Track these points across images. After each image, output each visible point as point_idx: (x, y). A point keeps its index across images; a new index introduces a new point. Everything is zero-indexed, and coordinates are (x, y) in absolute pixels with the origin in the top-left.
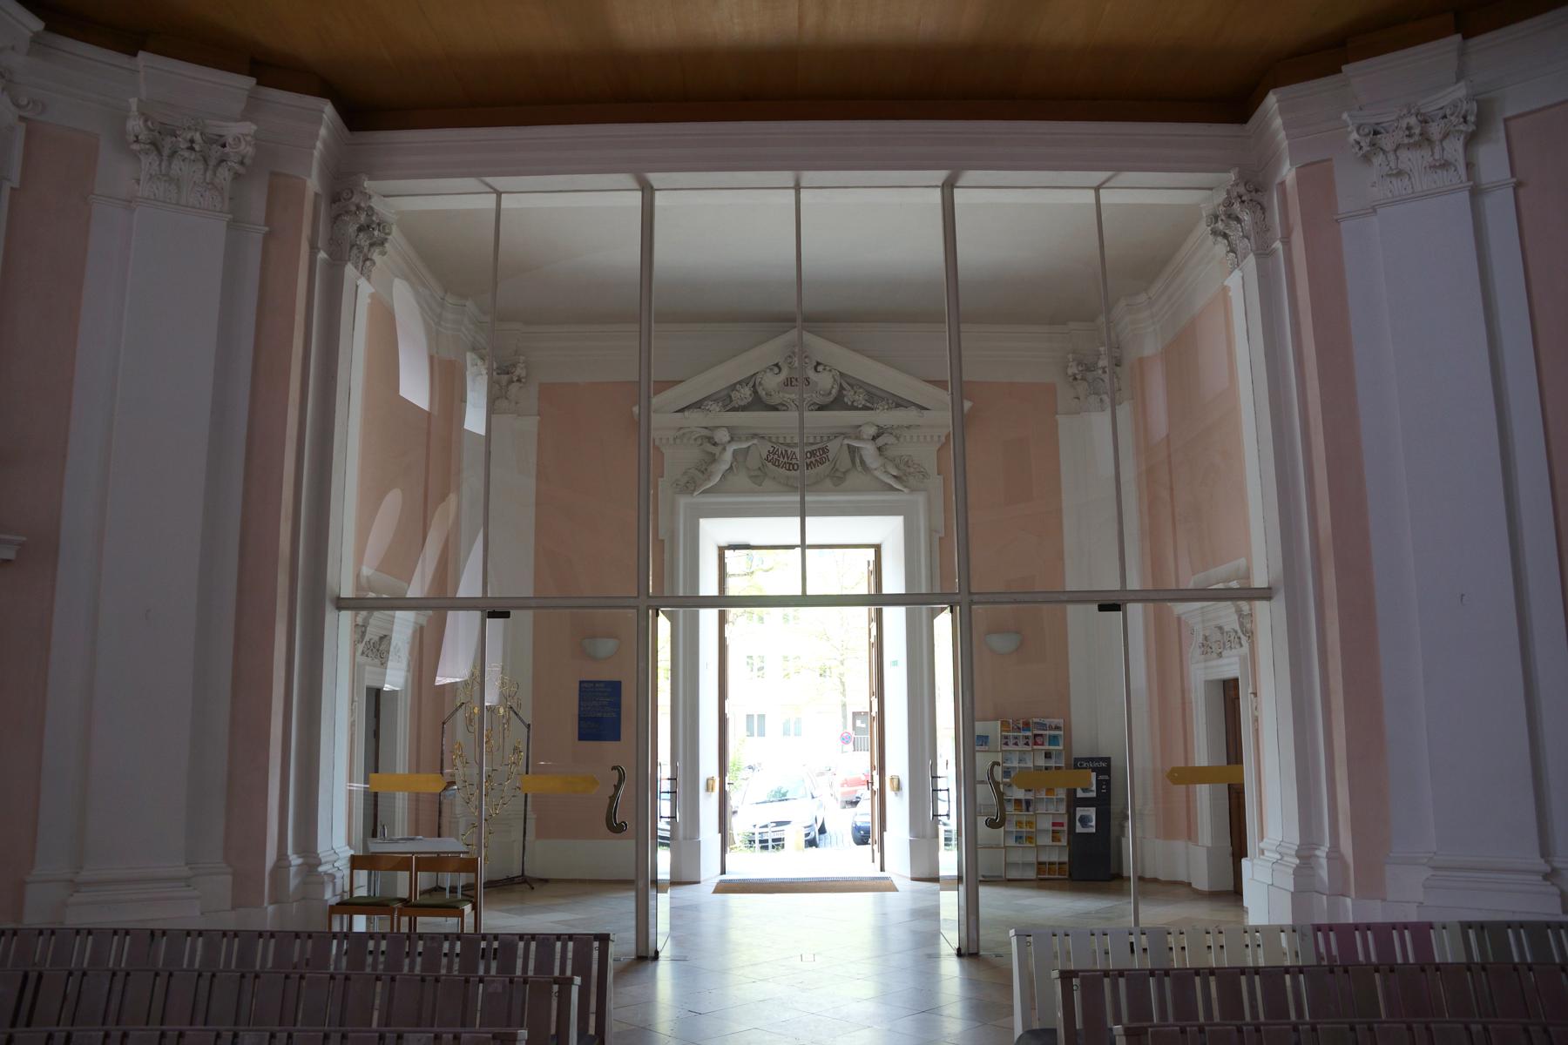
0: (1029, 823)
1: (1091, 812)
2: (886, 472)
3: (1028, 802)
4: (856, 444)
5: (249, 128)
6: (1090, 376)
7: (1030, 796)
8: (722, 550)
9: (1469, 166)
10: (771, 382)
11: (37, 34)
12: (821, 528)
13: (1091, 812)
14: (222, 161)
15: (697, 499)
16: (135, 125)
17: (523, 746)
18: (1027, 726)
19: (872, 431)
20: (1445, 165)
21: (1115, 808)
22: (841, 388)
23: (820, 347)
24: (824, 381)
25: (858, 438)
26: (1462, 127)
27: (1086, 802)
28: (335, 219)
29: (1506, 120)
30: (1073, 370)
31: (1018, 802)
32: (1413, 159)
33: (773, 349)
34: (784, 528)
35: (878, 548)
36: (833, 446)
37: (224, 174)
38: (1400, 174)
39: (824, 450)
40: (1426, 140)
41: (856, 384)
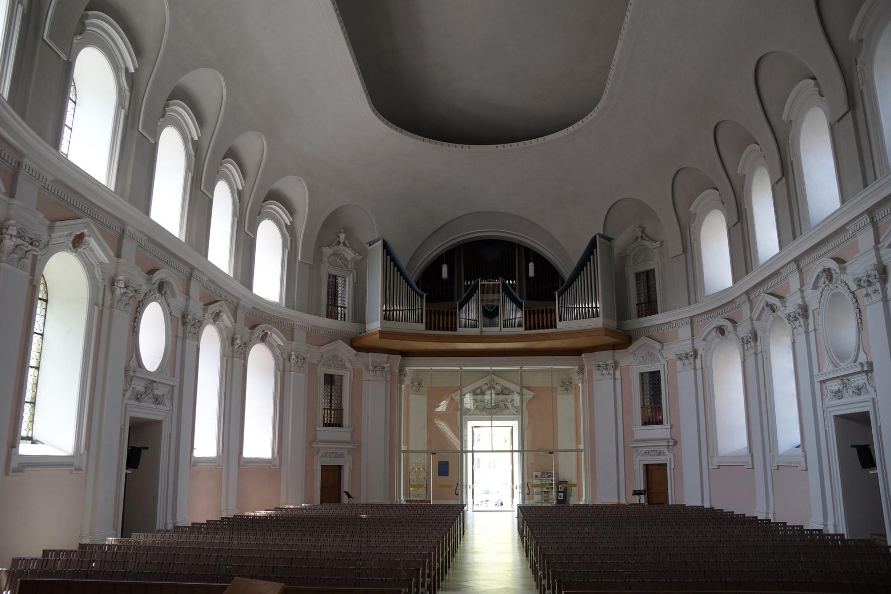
0: (548, 497)
1: (562, 494)
2: (514, 411)
3: (547, 492)
4: (506, 403)
5: (388, 365)
6: (565, 385)
7: (548, 490)
8: (473, 427)
9: (614, 374)
10: (485, 387)
11: (356, 354)
12: (495, 423)
13: (562, 494)
14: (384, 371)
15: (467, 416)
16: (371, 367)
17: (426, 478)
18: (547, 473)
19: (510, 400)
20: (610, 374)
21: (568, 493)
22: (503, 389)
23: (498, 379)
24: (498, 387)
25: (507, 402)
26: (612, 368)
27: (561, 492)
28: (400, 375)
29: (621, 367)
30: (560, 384)
31: (545, 492)
32: (605, 372)
33: (486, 380)
34: (488, 423)
35: (512, 427)
36: (501, 404)
37: (384, 373)
38: (603, 375)
39: (498, 405)
40: (607, 369)
41: (506, 388)
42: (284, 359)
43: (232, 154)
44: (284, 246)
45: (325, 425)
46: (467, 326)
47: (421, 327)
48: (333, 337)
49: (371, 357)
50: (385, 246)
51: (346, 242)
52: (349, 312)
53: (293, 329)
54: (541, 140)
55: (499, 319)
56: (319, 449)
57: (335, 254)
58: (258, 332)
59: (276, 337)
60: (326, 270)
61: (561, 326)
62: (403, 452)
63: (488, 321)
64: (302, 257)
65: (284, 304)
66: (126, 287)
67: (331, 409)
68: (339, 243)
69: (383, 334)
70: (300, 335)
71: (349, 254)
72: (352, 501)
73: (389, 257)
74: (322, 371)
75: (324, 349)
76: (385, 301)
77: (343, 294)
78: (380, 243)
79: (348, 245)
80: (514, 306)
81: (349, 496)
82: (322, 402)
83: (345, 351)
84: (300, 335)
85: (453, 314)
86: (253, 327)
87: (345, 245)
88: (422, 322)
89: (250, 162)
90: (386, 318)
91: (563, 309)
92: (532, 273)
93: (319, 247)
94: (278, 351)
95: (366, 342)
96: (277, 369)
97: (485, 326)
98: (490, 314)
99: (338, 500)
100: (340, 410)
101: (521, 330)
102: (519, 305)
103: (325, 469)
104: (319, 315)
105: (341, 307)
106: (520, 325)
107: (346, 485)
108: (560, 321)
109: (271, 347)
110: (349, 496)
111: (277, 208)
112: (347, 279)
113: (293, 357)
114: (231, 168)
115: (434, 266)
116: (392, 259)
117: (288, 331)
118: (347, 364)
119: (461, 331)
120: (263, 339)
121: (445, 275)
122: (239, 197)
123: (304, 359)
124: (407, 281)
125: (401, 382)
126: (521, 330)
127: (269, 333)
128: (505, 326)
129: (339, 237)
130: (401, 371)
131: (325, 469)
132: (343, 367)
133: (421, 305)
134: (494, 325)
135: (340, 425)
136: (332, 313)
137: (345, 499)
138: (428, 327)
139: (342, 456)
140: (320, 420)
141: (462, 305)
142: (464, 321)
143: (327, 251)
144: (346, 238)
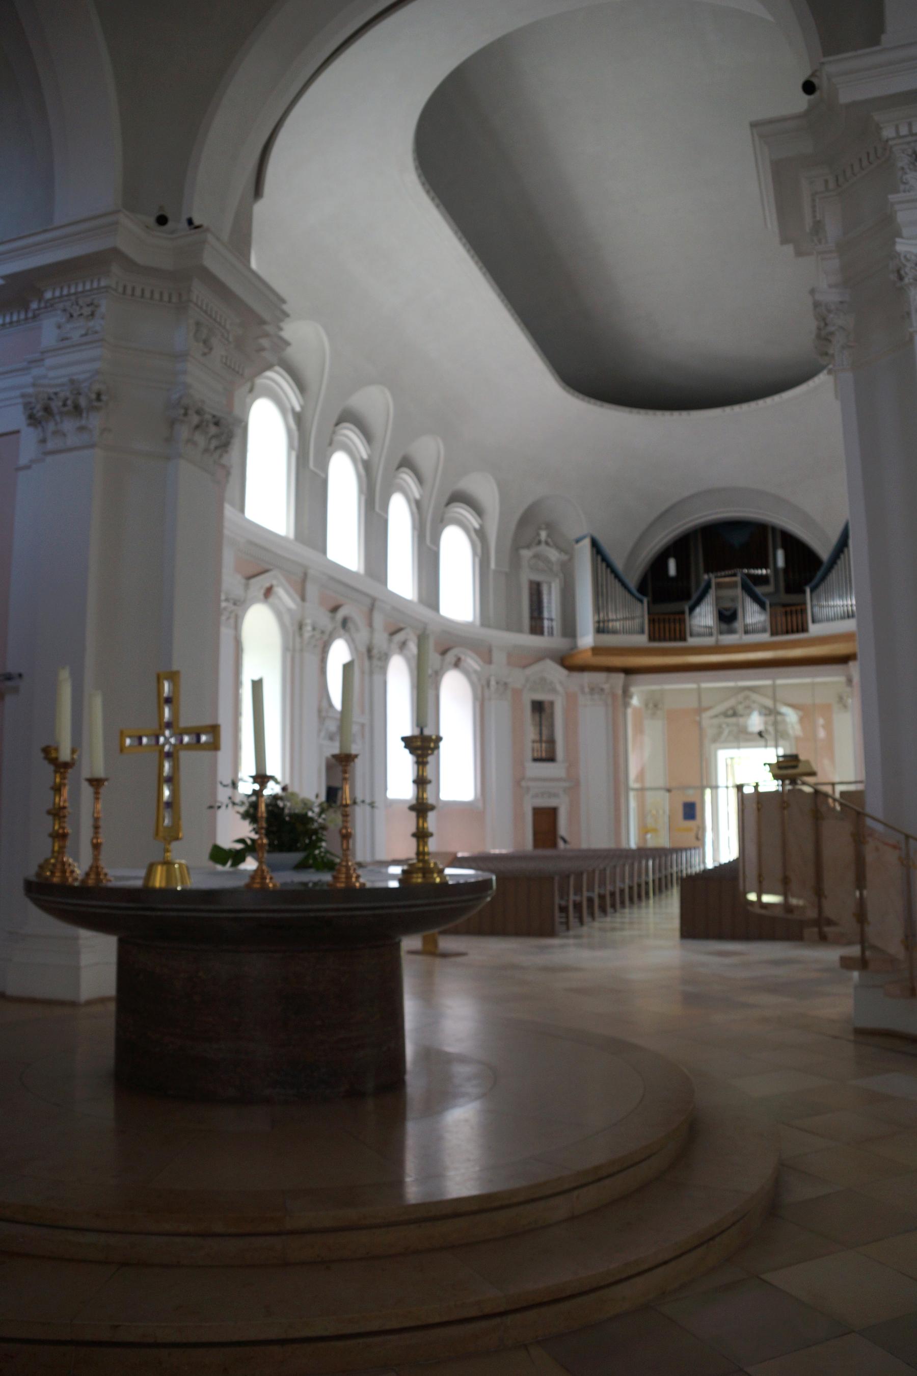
16: (587, 690)
23: (755, 696)
33: (740, 697)
42: (483, 687)
43: (406, 463)
44: (475, 553)
45: (535, 760)
46: (699, 635)
47: (642, 640)
48: (540, 656)
49: (587, 678)
50: (595, 544)
51: (549, 540)
52: (557, 625)
53: (490, 651)
54: (777, 398)
55: (738, 625)
56: (528, 789)
57: (536, 556)
58: (450, 657)
59: (472, 662)
60: (526, 576)
61: (814, 629)
62: (633, 789)
63: (724, 627)
64: (497, 564)
65: (478, 622)
66: (314, 629)
67: (541, 741)
68: (539, 543)
69: (596, 650)
70: (499, 657)
71: (553, 555)
72: (568, 846)
73: (599, 558)
74: (528, 698)
75: (529, 671)
76: (597, 609)
77: (549, 602)
78: (587, 542)
79: (551, 543)
80: (756, 607)
81: (565, 841)
82: (530, 733)
83: (555, 673)
84: (499, 657)
85: (682, 622)
86: (444, 653)
87: (547, 543)
88: (642, 632)
89: (426, 464)
90: (600, 630)
91: (816, 609)
92: (781, 563)
93: (516, 547)
94: (474, 677)
95: (579, 660)
96: (475, 698)
97: (721, 632)
98: (727, 618)
99: (554, 845)
100: (551, 742)
101: (765, 637)
102: (762, 605)
103: (538, 812)
104: (520, 630)
105: (548, 619)
106: (764, 630)
107: (563, 828)
108: (814, 621)
109: (467, 673)
110: (565, 841)
111: (462, 511)
112: (553, 585)
113: (493, 683)
114: (407, 478)
115: (659, 563)
116: (604, 559)
117: (485, 653)
118: (559, 688)
119: (692, 641)
120: (457, 664)
121: (672, 569)
122: (418, 507)
123: (506, 684)
124: (624, 585)
125: (626, 704)
126: (765, 637)
127: (463, 657)
128: (746, 632)
129: (538, 535)
130: (626, 694)
131: (538, 812)
132: (554, 691)
133: (640, 612)
134: (732, 631)
135: (551, 759)
136: (536, 628)
137: (561, 845)
138: (652, 638)
139: (556, 795)
140: (529, 755)
141: (692, 609)
142: (696, 629)
143: (526, 554)
144: (548, 536)
